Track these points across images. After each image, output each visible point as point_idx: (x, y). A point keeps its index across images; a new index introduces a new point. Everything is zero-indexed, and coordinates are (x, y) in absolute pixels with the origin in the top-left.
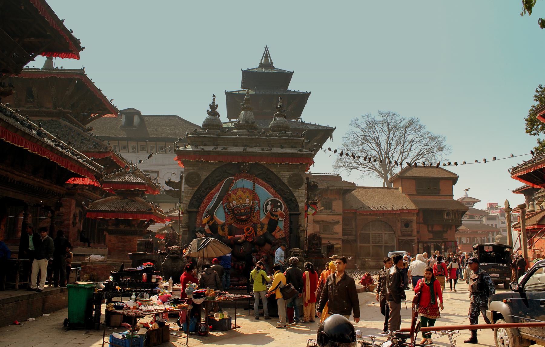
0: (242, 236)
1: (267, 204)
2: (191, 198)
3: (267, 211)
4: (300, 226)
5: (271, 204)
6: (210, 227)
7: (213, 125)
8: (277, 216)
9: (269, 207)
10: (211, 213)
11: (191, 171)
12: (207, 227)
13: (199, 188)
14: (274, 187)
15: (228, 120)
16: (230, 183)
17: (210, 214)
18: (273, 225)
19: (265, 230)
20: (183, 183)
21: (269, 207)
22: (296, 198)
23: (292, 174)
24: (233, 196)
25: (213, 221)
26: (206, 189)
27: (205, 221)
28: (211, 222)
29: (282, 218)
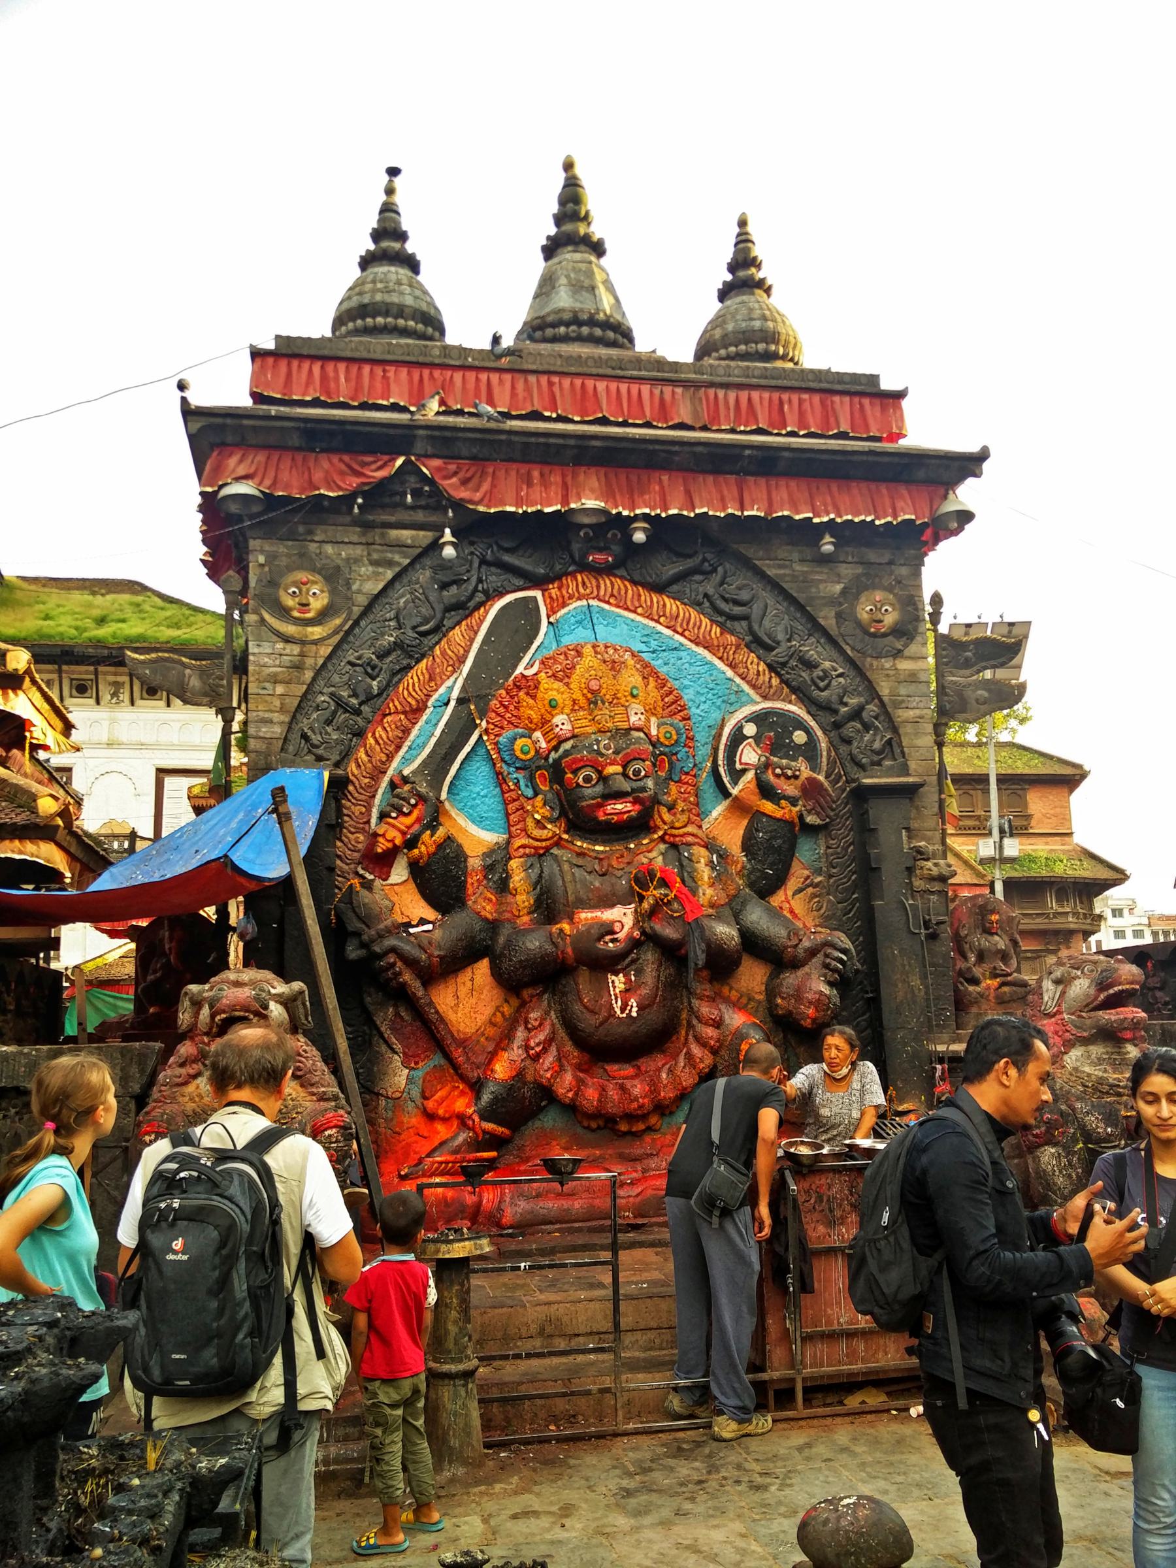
0: (622, 917)
1: (738, 738)
4: (921, 854)
5: (757, 738)
6: (417, 870)
7: (400, 311)
8: (793, 801)
16: (519, 628)
21: (749, 755)
24: (551, 689)
25: (441, 832)
26: (381, 656)
27: (392, 834)
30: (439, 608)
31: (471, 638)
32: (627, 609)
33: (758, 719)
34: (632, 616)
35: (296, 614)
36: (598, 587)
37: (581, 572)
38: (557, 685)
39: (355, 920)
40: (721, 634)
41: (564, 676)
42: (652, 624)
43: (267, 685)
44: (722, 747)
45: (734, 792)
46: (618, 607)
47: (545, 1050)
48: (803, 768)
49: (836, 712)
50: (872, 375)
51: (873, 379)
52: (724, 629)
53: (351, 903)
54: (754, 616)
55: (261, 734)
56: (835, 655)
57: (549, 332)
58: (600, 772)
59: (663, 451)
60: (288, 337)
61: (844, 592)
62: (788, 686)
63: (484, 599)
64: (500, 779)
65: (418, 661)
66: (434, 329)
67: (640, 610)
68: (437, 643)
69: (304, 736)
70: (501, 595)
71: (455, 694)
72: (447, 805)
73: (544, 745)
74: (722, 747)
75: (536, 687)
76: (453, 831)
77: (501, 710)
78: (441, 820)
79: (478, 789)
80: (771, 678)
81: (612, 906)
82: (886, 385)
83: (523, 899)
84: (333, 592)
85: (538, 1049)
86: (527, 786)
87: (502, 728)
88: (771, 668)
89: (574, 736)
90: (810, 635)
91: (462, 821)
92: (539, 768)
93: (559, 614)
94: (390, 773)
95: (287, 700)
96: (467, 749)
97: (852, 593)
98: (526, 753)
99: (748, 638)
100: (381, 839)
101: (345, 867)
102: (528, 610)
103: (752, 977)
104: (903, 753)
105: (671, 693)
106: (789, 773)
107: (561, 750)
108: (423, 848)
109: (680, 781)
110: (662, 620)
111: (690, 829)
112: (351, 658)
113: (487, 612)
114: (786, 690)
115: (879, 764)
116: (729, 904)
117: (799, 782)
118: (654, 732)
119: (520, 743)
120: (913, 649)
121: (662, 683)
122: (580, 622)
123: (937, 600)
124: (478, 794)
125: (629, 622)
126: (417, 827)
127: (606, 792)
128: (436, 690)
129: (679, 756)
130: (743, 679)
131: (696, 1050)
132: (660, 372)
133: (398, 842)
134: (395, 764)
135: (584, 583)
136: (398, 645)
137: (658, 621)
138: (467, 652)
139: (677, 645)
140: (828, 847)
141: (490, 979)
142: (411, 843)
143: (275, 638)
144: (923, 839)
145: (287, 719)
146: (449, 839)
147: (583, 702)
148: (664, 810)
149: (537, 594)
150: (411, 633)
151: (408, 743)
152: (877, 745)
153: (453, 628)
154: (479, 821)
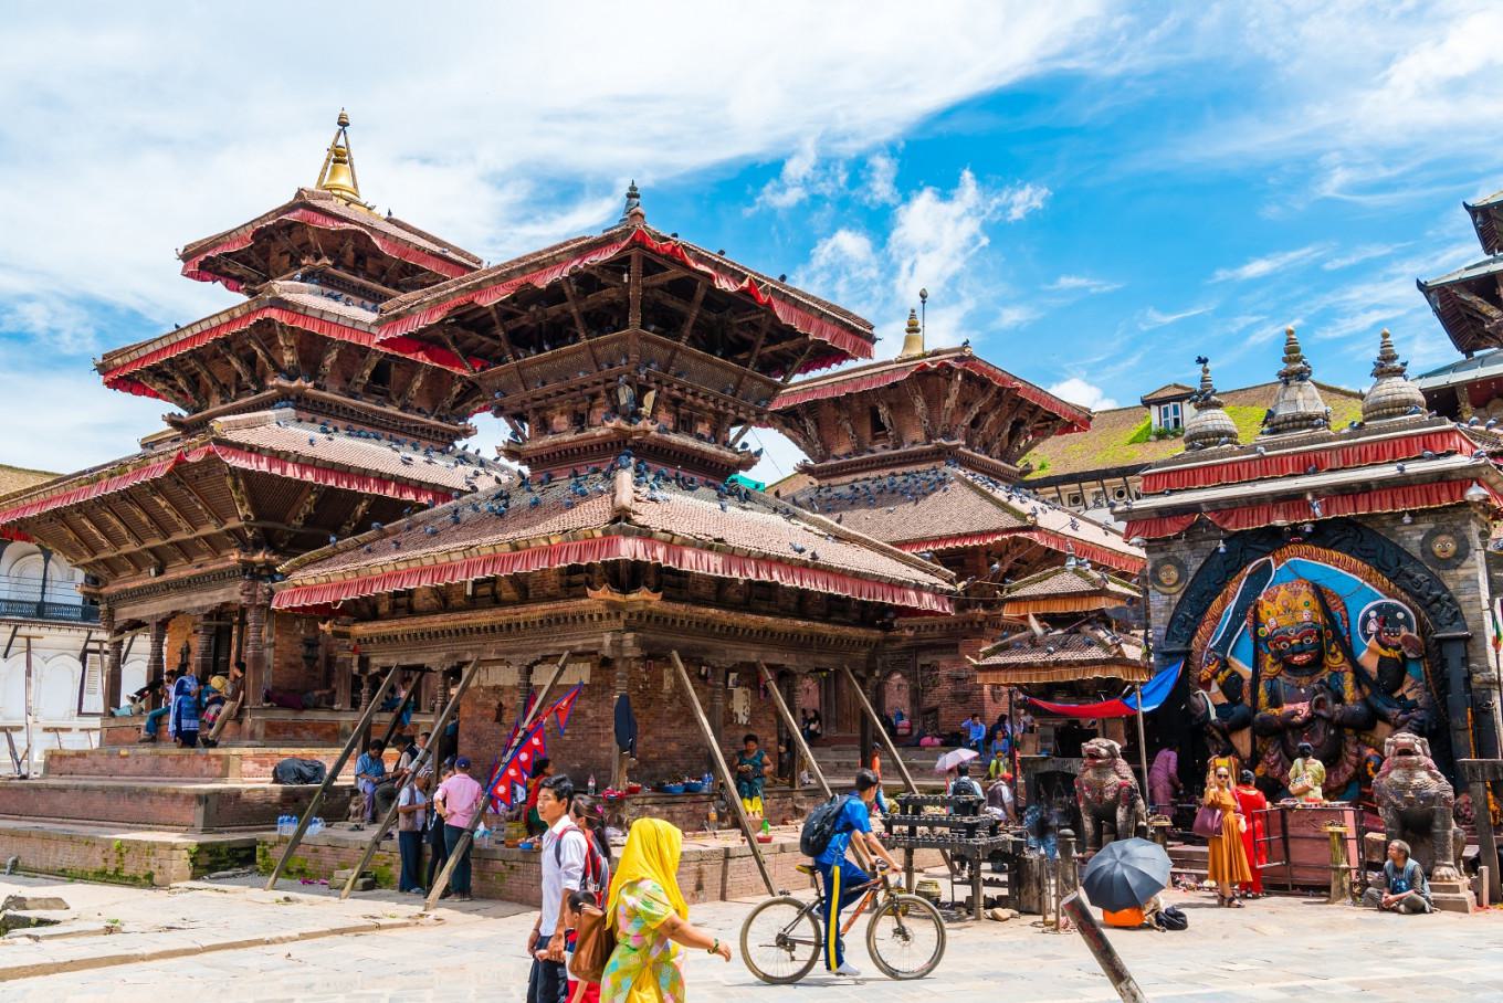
1: (1366, 619)
8: (1397, 648)
9: (1373, 627)
12: (1215, 688)
15: (1460, 357)
21: (1373, 627)
23: (1431, 530)
27: (1206, 673)
28: (1222, 676)
33: (1378, 608)
41: (1273, 600)
47: (1276, 765)
52: (1364, 562)
84: (1179, 572)
97: (1431, 535)
120: (1467, 563)
131: (1347, 766)
142: (1215, 676)
144: (1477, 662)
146: (1234, 672)
149: (1271, 558)
152: (1448, 615)
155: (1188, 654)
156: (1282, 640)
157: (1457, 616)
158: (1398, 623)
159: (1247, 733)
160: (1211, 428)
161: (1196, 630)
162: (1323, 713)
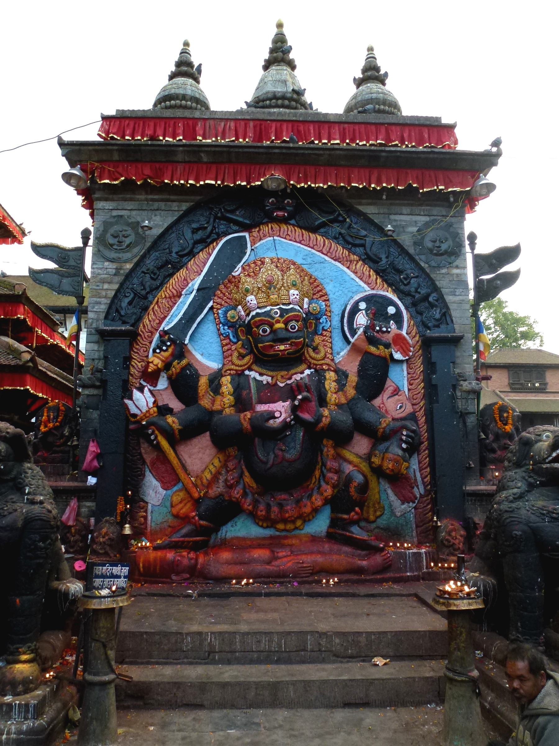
1: (355, 310)
2: (111, 294)
3: (353, 332)
4: (462, 377)
5: (367, 310)
7: (184, 97)
10: (176, 343)
11: (115, 213)
13: (137, 265)
14: (370, 260)
17: (173, 341)
18: (373, 376)
19: (351, 392)
20: (89, 252)
21: (361, 320)
22: (444, 291)
25: (184, 362)
26: (159, 268)
27: (156, 361)
29: (404, 353)
30: (191, 242)
31: (208, 258)
32: (296, 242)
33: (368, 299)
34: (299, 245)
35: (115, 247)
36: (280, 230)
37: (271, 222)
38: (248, 279)
39: (134, 407)
40: (349, 255)
42: (310, 249)
43: (98, 284)
44: (346, 315)
45: (352, 340)
46: (290, 240)
48: (393, 327)
49: (414, 297)
50: (437, 118)
51: (438, 119)
53: (131, 398)
54: (368, 245)
55: (95, 310)
56: (413, 266)
57: (261, 104)
58: (271, 325)
59: (314, 154)
60: (123, 111)
61: (418, 231)
62: (387, 283)
63: (216, 237)
64: (220, 335)
65: (178, 270)
66: (202, 106)
67: (303, 242)
68: (190, 260)
69: (117, 311)
70: (226, 235)
71: (196, 287)
72: (190, 347)
73: (243, 313)
74: (346, 315)
75: (239, 282)
76: (193, 361)
77: (221, 295)
78: (186, 354)
79: (208, 339)
80: (376, 279)
81: (274, 402)
82: (444, 121)
83: (229, 399)
85: (232, 482)
86: (234, 336)
87: (221, 305)
88: (377, 273)
89: (258, 308)
90: (400, 255)
91: (198, 357)
92: (240, 326)
93: (257, 245)
94: (161, 328)
95: (109, 292)
96: (202, 316)
98: (234, 317)
99: (363, 257)
100: (151, 365)
101: (134, 381)
102: (241, 244)
103: (361, 445)
104: (452, 321)
105: (318, 286)
106: (384, 329)
107: (251, 315)
108: (174, 369)
109: (322, 334)
110: (315, 247)
111: (327, 361)
112: (144, 269)
113: (217, 244)
114: (386, 286)
115: (438, 326)
116: (348, 404)
117: (391, 336)
118: (306, 306)
119: (230, 313)
120: (457, 263)
121: (313, 281)
122: (268, 249)
123: (472, 238)
124: (208, 341)
125: (296, 248)
126: (171, 359)
127: (275, 338)
128: (187, 285)
129: (321, 321)
130: (361, 279)
132: (324, 123)
133: (159, 366)
134: (163, 325)
135: (272, 228)
136: (167, 262)
137: (312, 248)
138: (205, 265)
139: (323, 260)
140: (408, 373)
141: (209, 443)
143: (103, 260)
145: (109, 302)
147: (264, 289)
148: (310, 350)
149: (247, 235)
150: (174, 255)
151: (171, 314)
152: (438, 316)
153: (199, 253)
154: (209, 357)
155: (133, 336)
156: (262, 323)
157: (446, 316)
158: (387, 318)
159: (205, 440)
160: (189, 92)
161: (145, 309)
162: (306, 416)
